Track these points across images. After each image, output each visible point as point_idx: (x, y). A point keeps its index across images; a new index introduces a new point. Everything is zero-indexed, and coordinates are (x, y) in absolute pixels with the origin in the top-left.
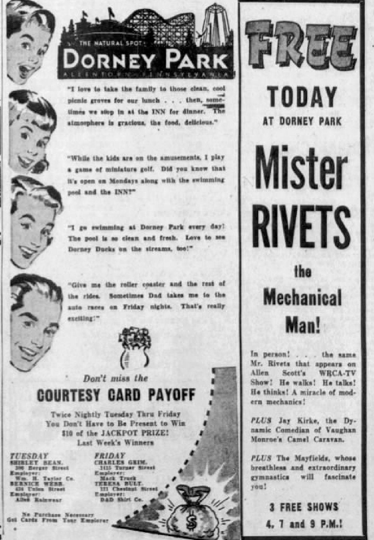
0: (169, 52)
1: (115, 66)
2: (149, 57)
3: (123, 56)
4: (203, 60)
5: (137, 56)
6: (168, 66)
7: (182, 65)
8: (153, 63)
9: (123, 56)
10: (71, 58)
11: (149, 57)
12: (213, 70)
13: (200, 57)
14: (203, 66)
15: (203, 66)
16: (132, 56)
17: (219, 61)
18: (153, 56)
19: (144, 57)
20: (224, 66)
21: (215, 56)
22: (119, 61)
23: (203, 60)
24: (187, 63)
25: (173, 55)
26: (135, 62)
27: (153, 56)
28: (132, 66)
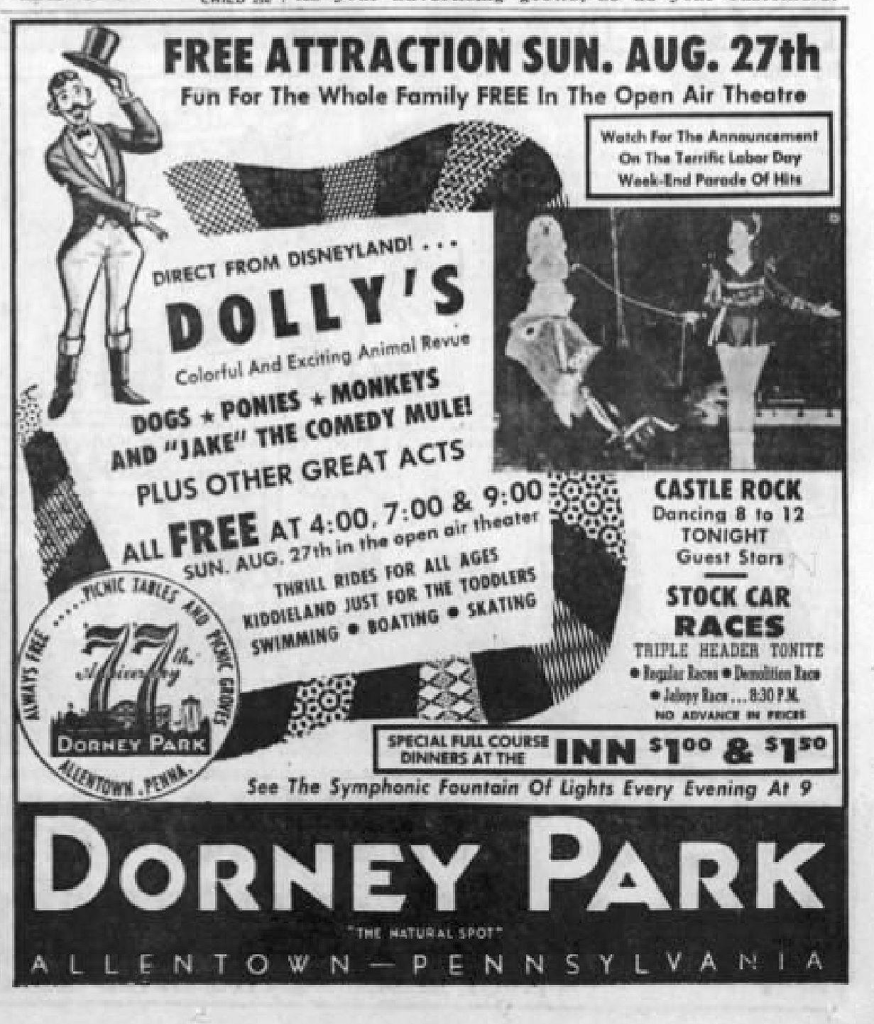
0: (541, 832)
1: (283, 901)
2: (445, 857)
3: (324, 854)
4: (709, 868)
5: (391, 853)
6: (539, 900)
7: (607, 895)
8: (461, 886)
9: (324, 854)
11: (445, 857)
13: (692, 853)
14: (704, 895)
15: (704, 895)
16: (364, 854)
17: (781, 871)
18: (466, 854)
19: (425, 854)
20: (806, 897)
21: (766, 851)
22: (303, 877)
23: (709, 868)
25: (565, 847)
26: (383, 878)
27: (466, 854)
28: (364, 901)
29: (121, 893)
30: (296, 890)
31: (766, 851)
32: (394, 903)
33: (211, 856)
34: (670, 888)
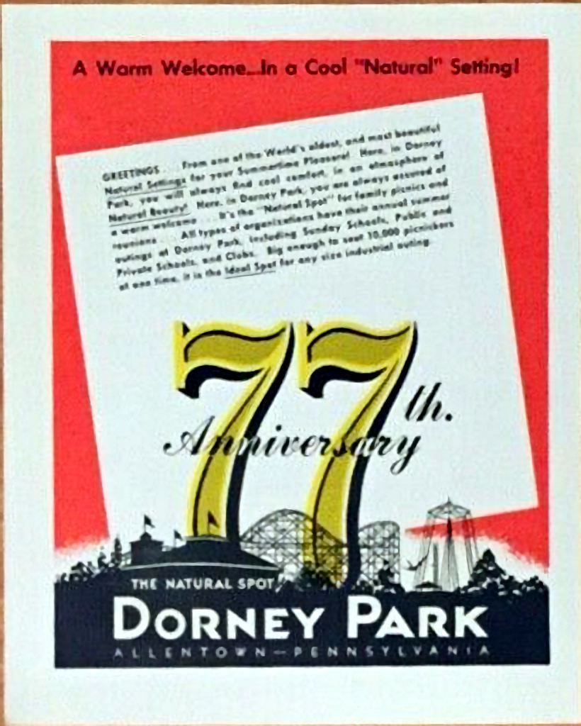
0: (354, 601)
1: (232, 634)
2: (308, 614)
3: (251, 613)
5: (283, 612)
6: (353, 633)
8: (317, 627)
9: (251, 613)
10: (131, 618)
11: (308, 614)
12: (453, 640)
13: (424, 612)
14: (431, 631)
15: (431, 631)
16: (270, 613)
18: (318, 613)
19: (298, 612)
20: (479, 632)
21: (459, 611)
23: (432, 618)
24: (395, 624)
27: (318, 613)
28: (270, 634)
29: (156, 635)
30: (239, 630)
31: (459, 611)
32: (284, 635)
33: (197, 613)
34: (414, 625)
